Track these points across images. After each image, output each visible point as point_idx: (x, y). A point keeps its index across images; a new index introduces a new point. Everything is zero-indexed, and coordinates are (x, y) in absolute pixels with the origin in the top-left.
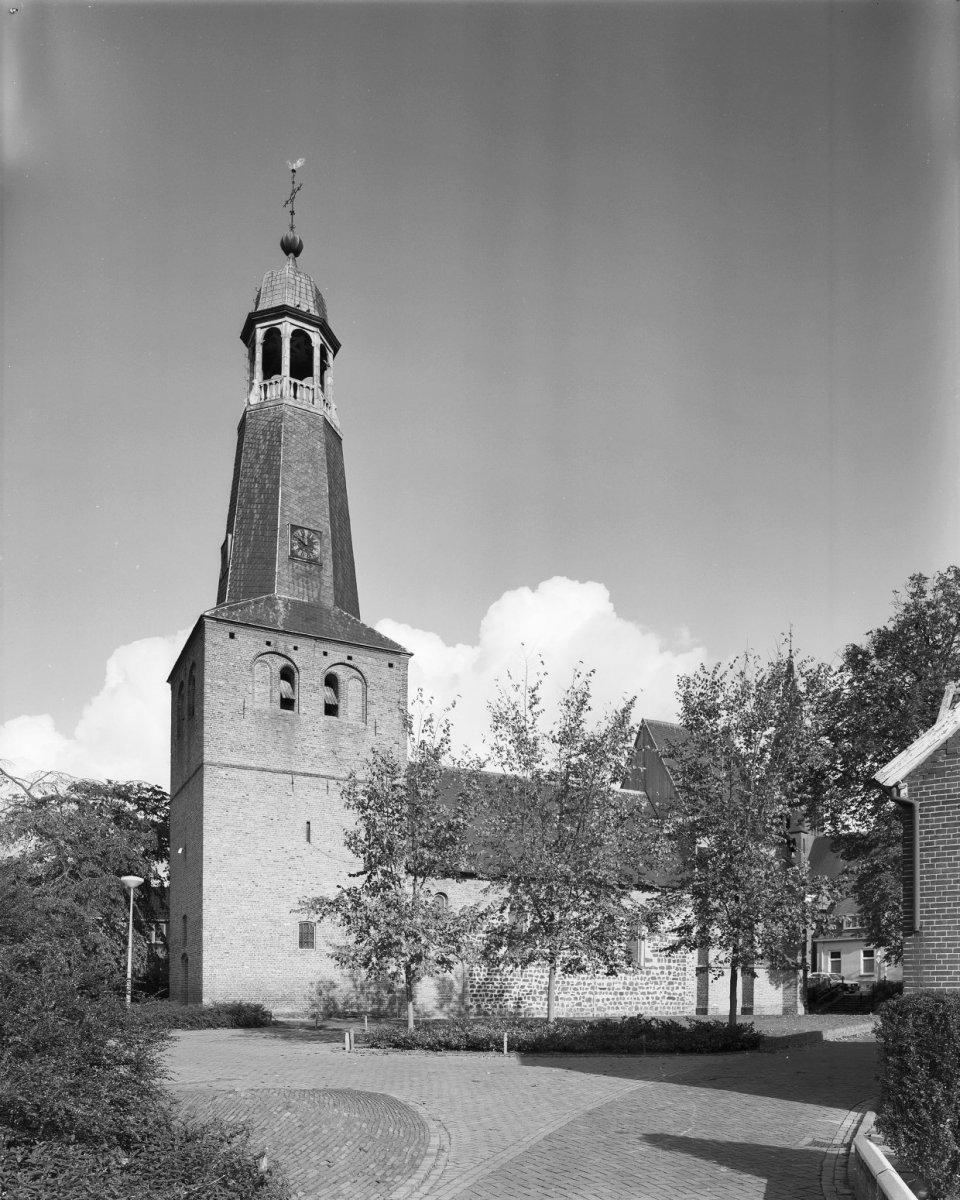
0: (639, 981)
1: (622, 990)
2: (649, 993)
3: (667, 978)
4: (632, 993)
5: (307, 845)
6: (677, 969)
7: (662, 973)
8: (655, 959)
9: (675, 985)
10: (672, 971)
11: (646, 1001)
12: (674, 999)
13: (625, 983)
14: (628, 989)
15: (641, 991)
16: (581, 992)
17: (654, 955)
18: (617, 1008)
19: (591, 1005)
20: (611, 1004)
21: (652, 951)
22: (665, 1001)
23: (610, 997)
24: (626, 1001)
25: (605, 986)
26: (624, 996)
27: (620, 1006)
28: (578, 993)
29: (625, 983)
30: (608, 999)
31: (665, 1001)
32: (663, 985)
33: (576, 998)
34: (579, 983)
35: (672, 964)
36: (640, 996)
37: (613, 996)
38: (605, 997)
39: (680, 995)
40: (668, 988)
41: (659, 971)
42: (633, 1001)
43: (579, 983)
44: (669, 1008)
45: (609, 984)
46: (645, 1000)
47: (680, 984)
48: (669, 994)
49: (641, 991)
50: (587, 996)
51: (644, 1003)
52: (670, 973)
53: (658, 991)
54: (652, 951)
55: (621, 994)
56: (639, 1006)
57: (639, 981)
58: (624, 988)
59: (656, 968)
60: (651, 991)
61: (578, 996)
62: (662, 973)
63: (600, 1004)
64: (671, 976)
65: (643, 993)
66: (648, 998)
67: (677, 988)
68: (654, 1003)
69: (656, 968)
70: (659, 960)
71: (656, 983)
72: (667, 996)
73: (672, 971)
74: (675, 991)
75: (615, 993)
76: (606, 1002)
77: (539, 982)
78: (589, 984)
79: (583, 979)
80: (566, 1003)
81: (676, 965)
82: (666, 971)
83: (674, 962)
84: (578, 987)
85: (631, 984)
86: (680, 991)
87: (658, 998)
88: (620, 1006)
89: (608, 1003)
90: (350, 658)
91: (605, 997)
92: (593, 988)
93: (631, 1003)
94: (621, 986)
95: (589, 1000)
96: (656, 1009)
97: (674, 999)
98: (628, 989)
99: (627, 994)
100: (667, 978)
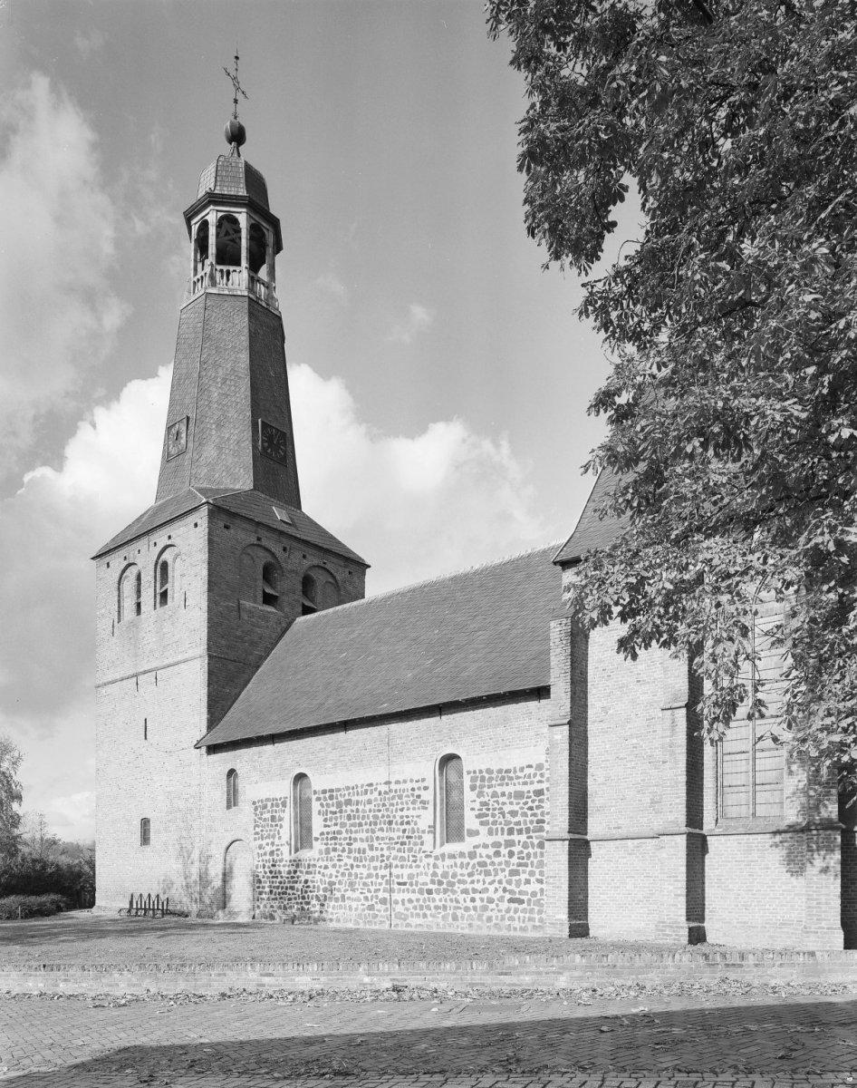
0: (459, 871)
1: (431, 886)
2: (475, 891)
3: (507, 863)
4: (445, 891)
5: (146, 743)
6: (525, 846)
7: (497, 854)
8: (483, 830)
9: (523, 877)
10: (516, 849)
11: (471, 905)
12: (521, 902)
13: (435, 874)
14: (440, 883)
15: (462, 887)
16: (372, 888)
17: (482, 823)
18: (425, 916)
19: (386, 910)
20: (415, 908)
21: (477, 817)
22: (504, 905)
23: (414, 897)
24: (438, 903)
25: (405, 879)
26: (434, 895)
27: (428, 912)
28: (369, 891)
29: (435, 874)
30: (410, 901)
31: (504, 905)
32: (501, 876)
33: (366, 898)
34: (369, 876)
35: (515, 837)
36: (461, 897)
37: (417, 895)
38: (406, 896)
39: (534, 894)
40: (509, 882)
41: (491, 851)
42: (448, 904)
43: (369, 876)
44: (511, 919)
45: (411, 876)
46: (471, 905)
47: (532, 873)
48: (511, 892)
49: (462, 887)
50: (381, 895)
51: (467, 909)
52: (511, 854)
53: (492, 888)
54: (477, 817)
55: (429, 892)
56: (459, 913)
57: (459, 871)
58: (433, 882)
59: (486, 846)
60: (479, 886)
61: (369, 895)
62: (497, 854)
63: (399, 908)
64: (515, 860)
65: (465, 891)
66: (473, 900)
67: (528, 882)
68: (485, 908)
69: (486, 846)
70: (490, 833)
71: (488, 873)
72: (508, 896)
73: (516, 849)
74: (523, 888)
75: (421, 892)
76: (407, 905)
77: (323, 875)
78: (383, 877)
79: (375, 868)
80: (354, 905)
81: (523, 838)
82: (504, 851)
83: (520, 832)
84: (370, 880)
85: (445, 875)
86: (535, 887)
87: (491, 901)
88: (428, 912)
89: (410, 906)
90: (259, 539)
91: (406, 896)
92: (388, 882)
93: (445, 907)
94: (428, 879)
95: (383, 901)
96: (489, 919)
97: (521, 902)
98: (440, 883)
99: (438, 892)
100: (507, 863)
